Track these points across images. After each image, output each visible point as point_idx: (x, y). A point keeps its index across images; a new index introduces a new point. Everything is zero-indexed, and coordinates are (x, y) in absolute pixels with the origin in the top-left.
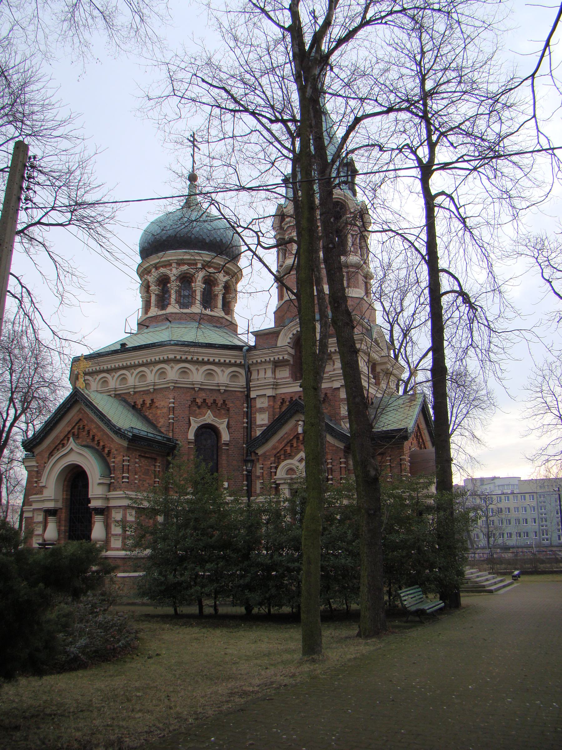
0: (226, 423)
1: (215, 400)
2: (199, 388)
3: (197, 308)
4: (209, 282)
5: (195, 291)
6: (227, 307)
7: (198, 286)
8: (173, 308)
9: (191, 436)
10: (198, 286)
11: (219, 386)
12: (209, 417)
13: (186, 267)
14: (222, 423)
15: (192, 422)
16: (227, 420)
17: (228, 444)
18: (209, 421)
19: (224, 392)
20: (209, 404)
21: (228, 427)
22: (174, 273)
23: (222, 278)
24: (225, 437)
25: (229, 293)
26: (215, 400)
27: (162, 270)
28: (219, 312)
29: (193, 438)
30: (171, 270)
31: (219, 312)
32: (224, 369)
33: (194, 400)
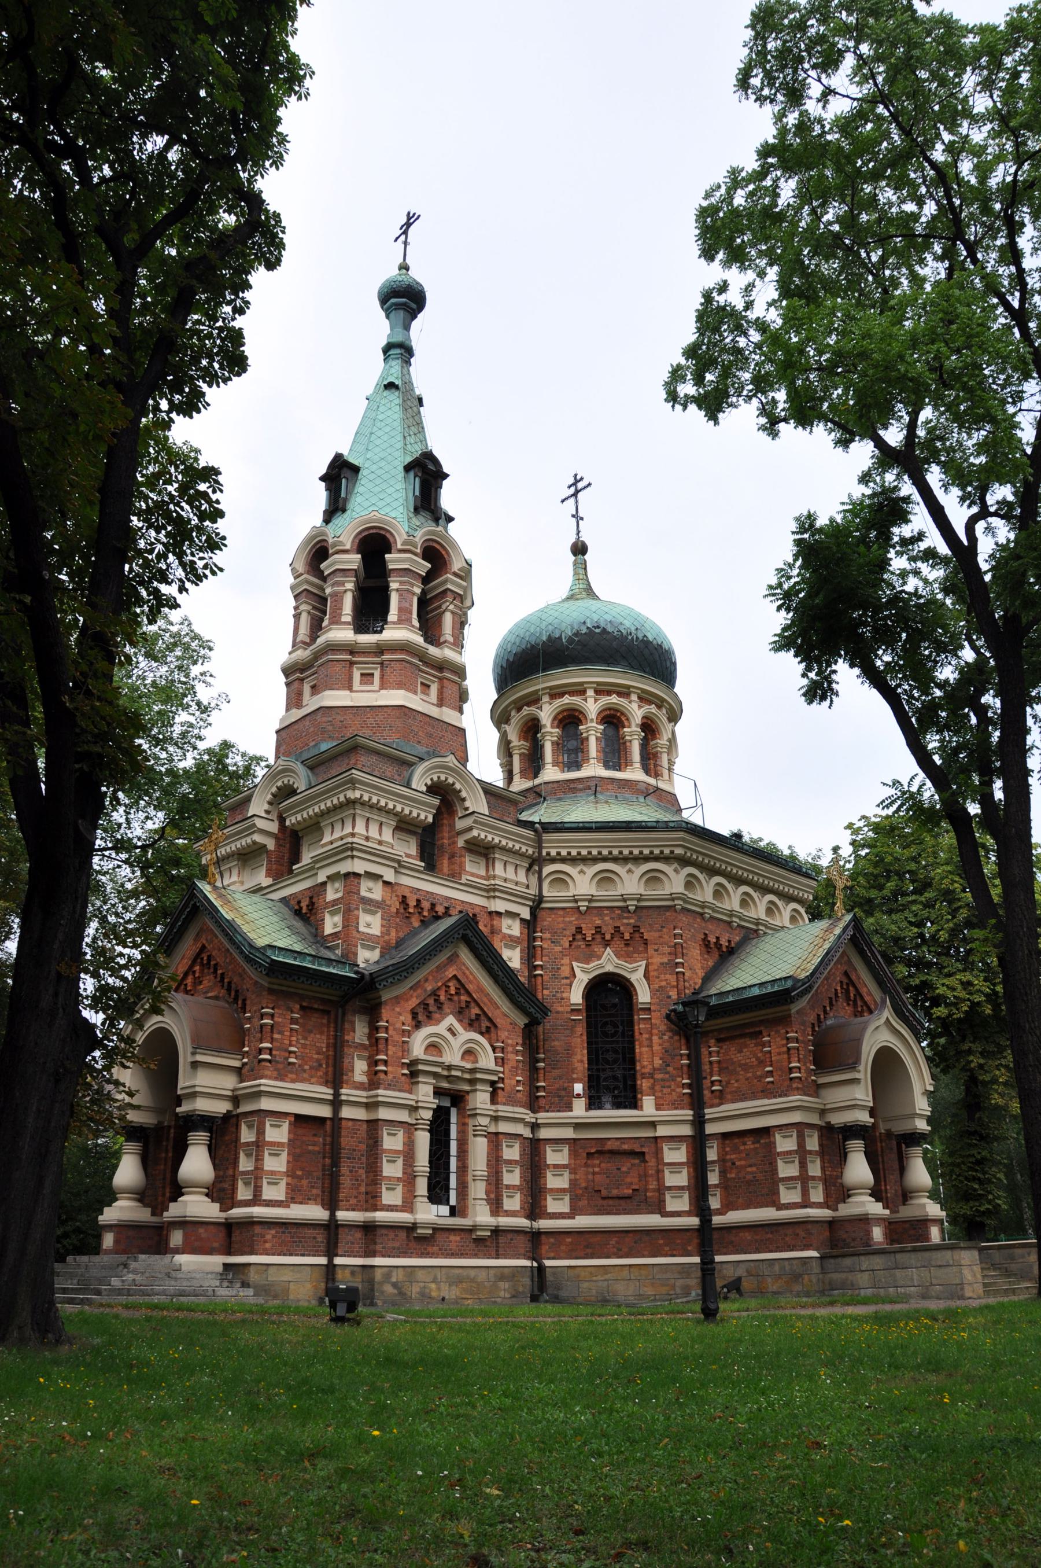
0: (642, 970)
1: (617, 929)
2: (588, 907)
3: (593, 769)
4: (613, 719)
5: (587, 739)
6: (650, 761)
7: (593, 731)
8: (551, 773)
9: (576, 996)
10: (593, 731)
11: (625, 900)
12: (609, 962)
13: (567, 700)
14: (635, 970)
15: (577, 971)
16: (644, 962)
17: (649, 1009)
18: (609, 968)
19: (635, 911)
20: (608, 937)
21: (646, 976)
22: (546, 713)
23: (636, 712)
24: (644, 995)
25: (654, 738)
26: (617, 929)
27: (526, 711)
28: (635, 773)
29: (580, 1001)
30: (541, 708)
31: (635, 773)
32: (633, 868)
33: (579, 930)
